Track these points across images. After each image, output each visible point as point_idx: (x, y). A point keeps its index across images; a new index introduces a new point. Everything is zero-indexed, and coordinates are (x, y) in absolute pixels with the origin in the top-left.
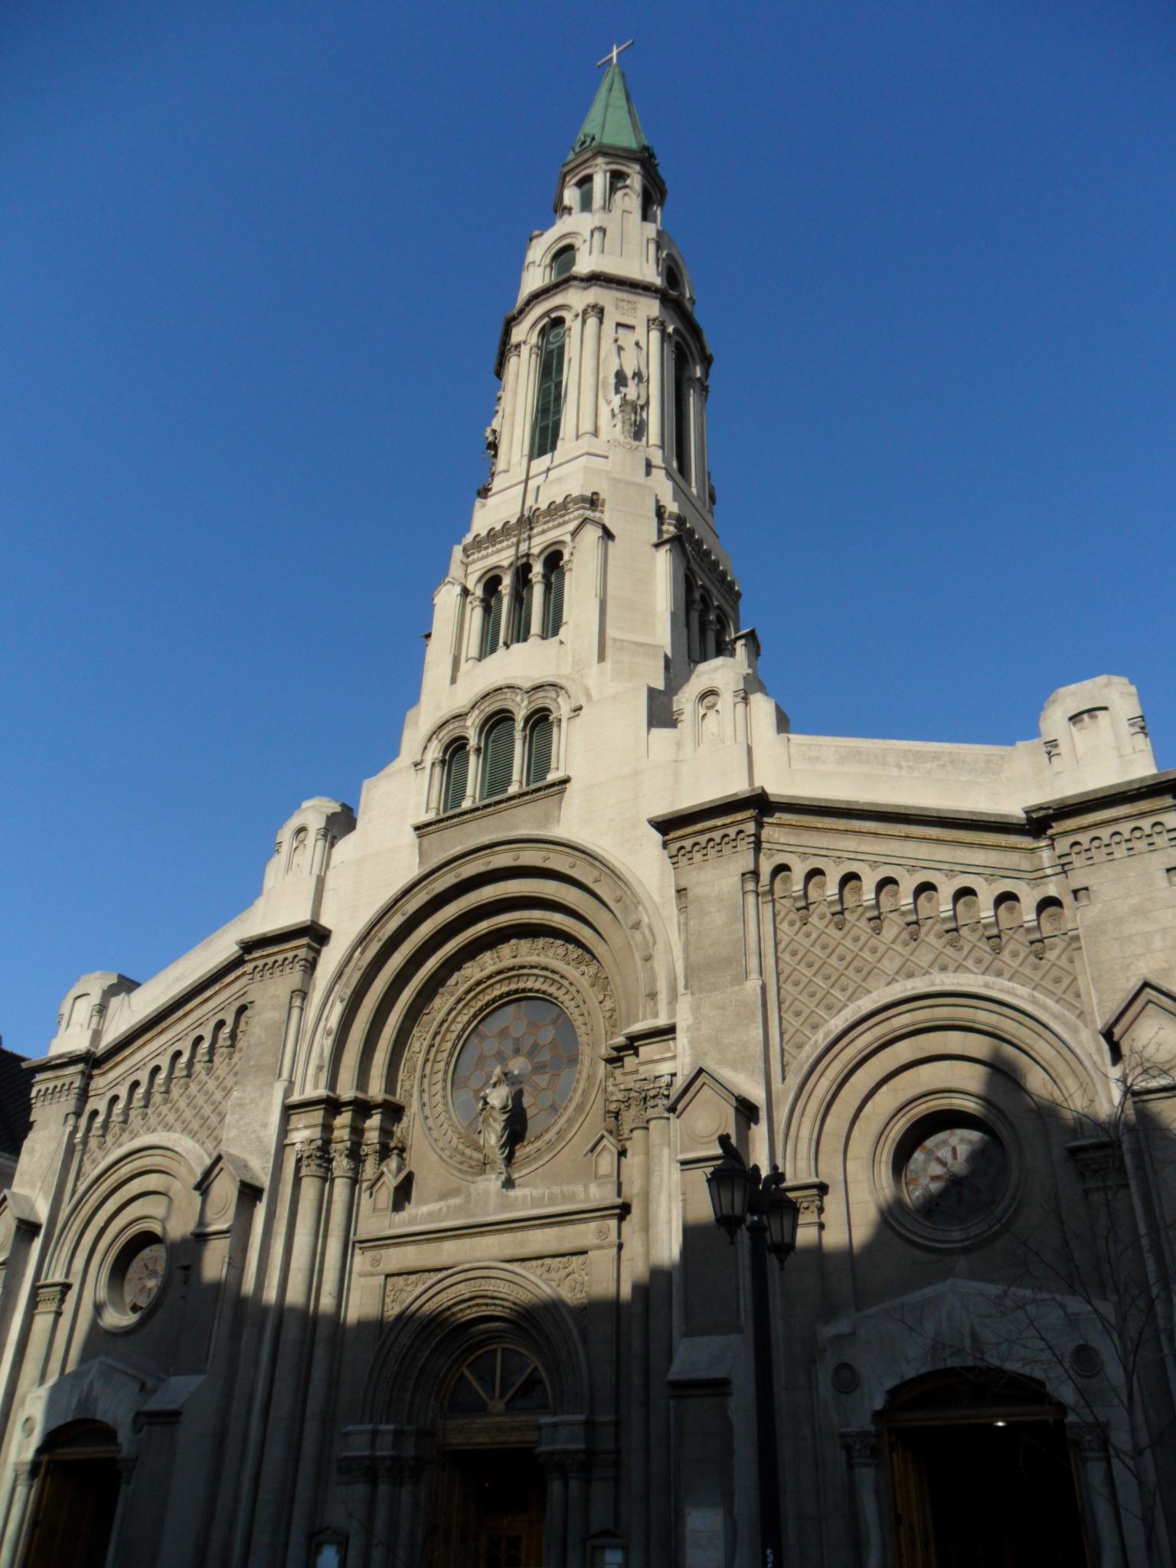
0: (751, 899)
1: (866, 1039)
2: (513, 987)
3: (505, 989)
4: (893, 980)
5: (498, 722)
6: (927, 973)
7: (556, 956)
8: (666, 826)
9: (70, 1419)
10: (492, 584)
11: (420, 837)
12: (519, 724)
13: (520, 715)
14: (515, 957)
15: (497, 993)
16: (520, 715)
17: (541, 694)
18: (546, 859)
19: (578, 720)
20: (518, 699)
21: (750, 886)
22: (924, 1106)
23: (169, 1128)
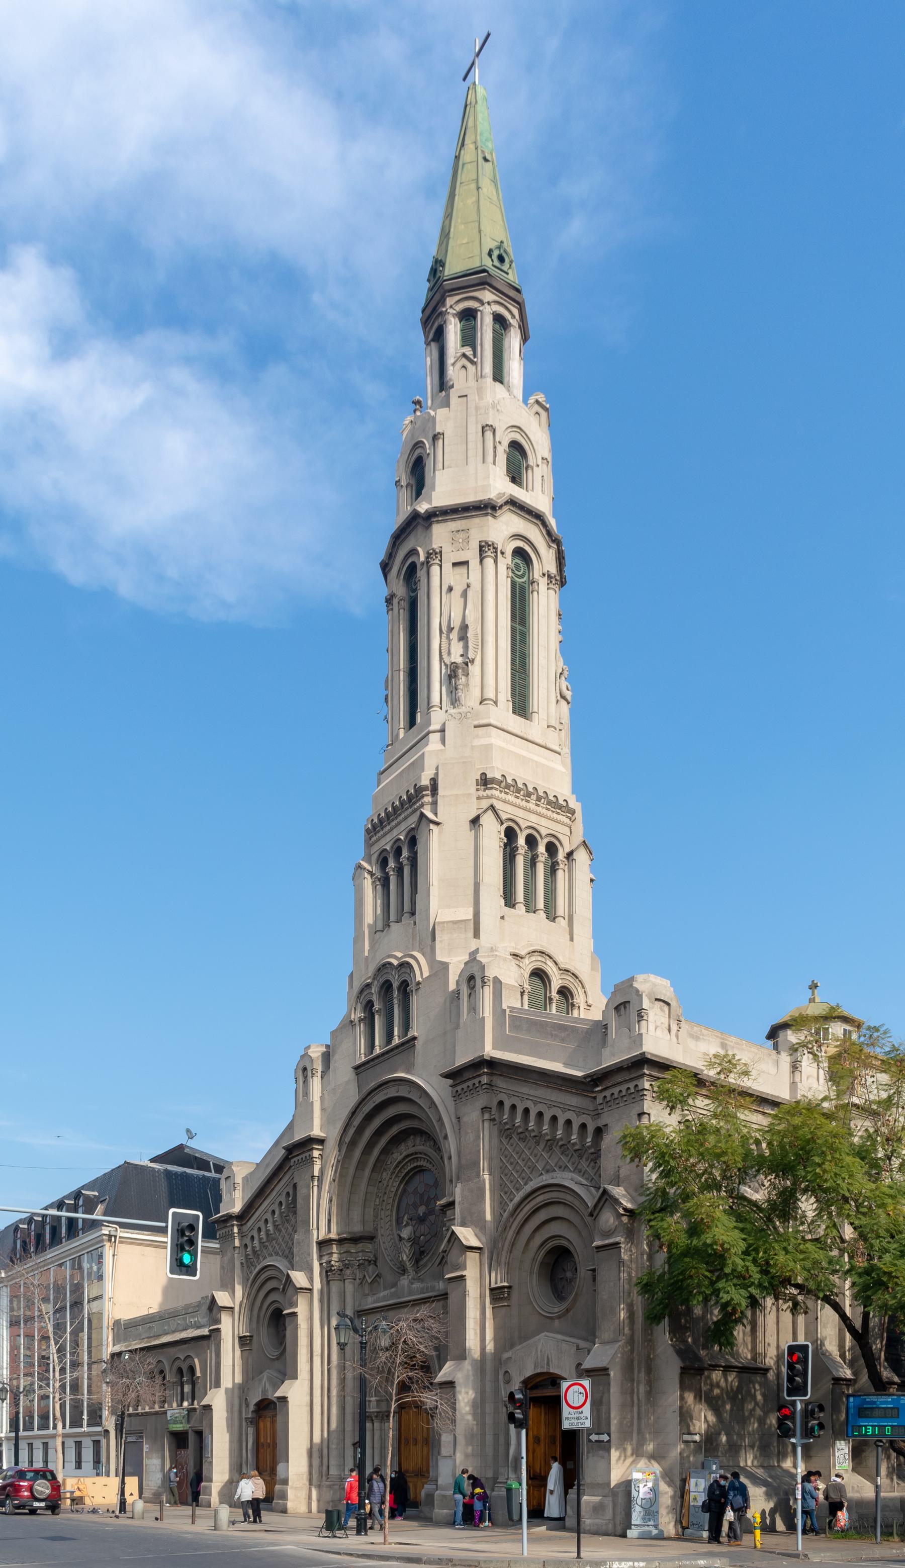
0: (486, 1124)
1: (527, 1209)
2: (415, 1164)
3: (412, 1166)
4: (542, 1174)
5: (387, 987)
6: (554, 1170)
7: (430, 1147)
8: (454, 1075)
9: (260, 1398)
10: (384, 863)
11: (357, 1074)
12: (396, 993)
13: (395, 985)
14: (414, 1146)
15: (409, 1168)
16: (395, 985)
17: (403, 970)
18: (409, 1092)
19: (420, 991)
20: (393, 973)
21: (487, 1116)
22: (551, 1244)
23: (277, 1254)
